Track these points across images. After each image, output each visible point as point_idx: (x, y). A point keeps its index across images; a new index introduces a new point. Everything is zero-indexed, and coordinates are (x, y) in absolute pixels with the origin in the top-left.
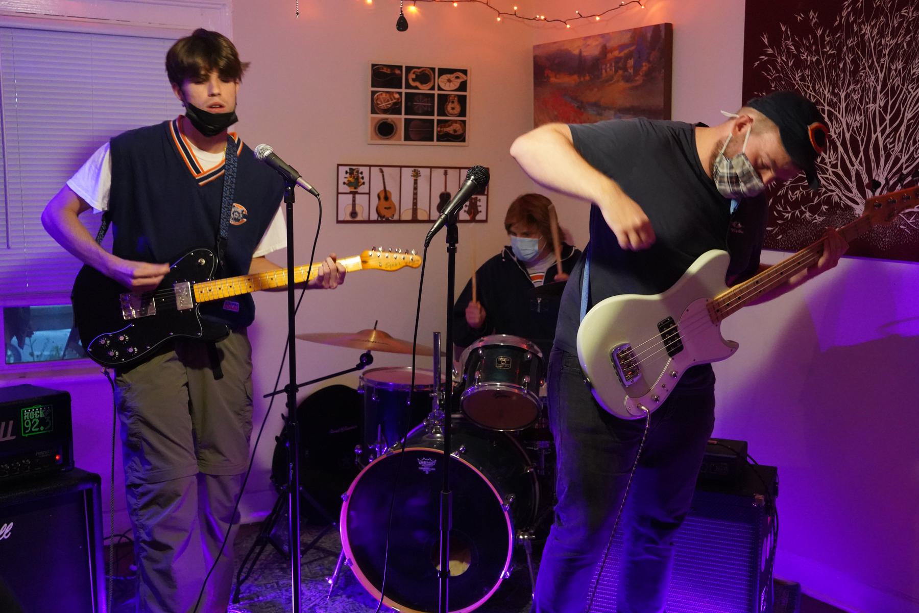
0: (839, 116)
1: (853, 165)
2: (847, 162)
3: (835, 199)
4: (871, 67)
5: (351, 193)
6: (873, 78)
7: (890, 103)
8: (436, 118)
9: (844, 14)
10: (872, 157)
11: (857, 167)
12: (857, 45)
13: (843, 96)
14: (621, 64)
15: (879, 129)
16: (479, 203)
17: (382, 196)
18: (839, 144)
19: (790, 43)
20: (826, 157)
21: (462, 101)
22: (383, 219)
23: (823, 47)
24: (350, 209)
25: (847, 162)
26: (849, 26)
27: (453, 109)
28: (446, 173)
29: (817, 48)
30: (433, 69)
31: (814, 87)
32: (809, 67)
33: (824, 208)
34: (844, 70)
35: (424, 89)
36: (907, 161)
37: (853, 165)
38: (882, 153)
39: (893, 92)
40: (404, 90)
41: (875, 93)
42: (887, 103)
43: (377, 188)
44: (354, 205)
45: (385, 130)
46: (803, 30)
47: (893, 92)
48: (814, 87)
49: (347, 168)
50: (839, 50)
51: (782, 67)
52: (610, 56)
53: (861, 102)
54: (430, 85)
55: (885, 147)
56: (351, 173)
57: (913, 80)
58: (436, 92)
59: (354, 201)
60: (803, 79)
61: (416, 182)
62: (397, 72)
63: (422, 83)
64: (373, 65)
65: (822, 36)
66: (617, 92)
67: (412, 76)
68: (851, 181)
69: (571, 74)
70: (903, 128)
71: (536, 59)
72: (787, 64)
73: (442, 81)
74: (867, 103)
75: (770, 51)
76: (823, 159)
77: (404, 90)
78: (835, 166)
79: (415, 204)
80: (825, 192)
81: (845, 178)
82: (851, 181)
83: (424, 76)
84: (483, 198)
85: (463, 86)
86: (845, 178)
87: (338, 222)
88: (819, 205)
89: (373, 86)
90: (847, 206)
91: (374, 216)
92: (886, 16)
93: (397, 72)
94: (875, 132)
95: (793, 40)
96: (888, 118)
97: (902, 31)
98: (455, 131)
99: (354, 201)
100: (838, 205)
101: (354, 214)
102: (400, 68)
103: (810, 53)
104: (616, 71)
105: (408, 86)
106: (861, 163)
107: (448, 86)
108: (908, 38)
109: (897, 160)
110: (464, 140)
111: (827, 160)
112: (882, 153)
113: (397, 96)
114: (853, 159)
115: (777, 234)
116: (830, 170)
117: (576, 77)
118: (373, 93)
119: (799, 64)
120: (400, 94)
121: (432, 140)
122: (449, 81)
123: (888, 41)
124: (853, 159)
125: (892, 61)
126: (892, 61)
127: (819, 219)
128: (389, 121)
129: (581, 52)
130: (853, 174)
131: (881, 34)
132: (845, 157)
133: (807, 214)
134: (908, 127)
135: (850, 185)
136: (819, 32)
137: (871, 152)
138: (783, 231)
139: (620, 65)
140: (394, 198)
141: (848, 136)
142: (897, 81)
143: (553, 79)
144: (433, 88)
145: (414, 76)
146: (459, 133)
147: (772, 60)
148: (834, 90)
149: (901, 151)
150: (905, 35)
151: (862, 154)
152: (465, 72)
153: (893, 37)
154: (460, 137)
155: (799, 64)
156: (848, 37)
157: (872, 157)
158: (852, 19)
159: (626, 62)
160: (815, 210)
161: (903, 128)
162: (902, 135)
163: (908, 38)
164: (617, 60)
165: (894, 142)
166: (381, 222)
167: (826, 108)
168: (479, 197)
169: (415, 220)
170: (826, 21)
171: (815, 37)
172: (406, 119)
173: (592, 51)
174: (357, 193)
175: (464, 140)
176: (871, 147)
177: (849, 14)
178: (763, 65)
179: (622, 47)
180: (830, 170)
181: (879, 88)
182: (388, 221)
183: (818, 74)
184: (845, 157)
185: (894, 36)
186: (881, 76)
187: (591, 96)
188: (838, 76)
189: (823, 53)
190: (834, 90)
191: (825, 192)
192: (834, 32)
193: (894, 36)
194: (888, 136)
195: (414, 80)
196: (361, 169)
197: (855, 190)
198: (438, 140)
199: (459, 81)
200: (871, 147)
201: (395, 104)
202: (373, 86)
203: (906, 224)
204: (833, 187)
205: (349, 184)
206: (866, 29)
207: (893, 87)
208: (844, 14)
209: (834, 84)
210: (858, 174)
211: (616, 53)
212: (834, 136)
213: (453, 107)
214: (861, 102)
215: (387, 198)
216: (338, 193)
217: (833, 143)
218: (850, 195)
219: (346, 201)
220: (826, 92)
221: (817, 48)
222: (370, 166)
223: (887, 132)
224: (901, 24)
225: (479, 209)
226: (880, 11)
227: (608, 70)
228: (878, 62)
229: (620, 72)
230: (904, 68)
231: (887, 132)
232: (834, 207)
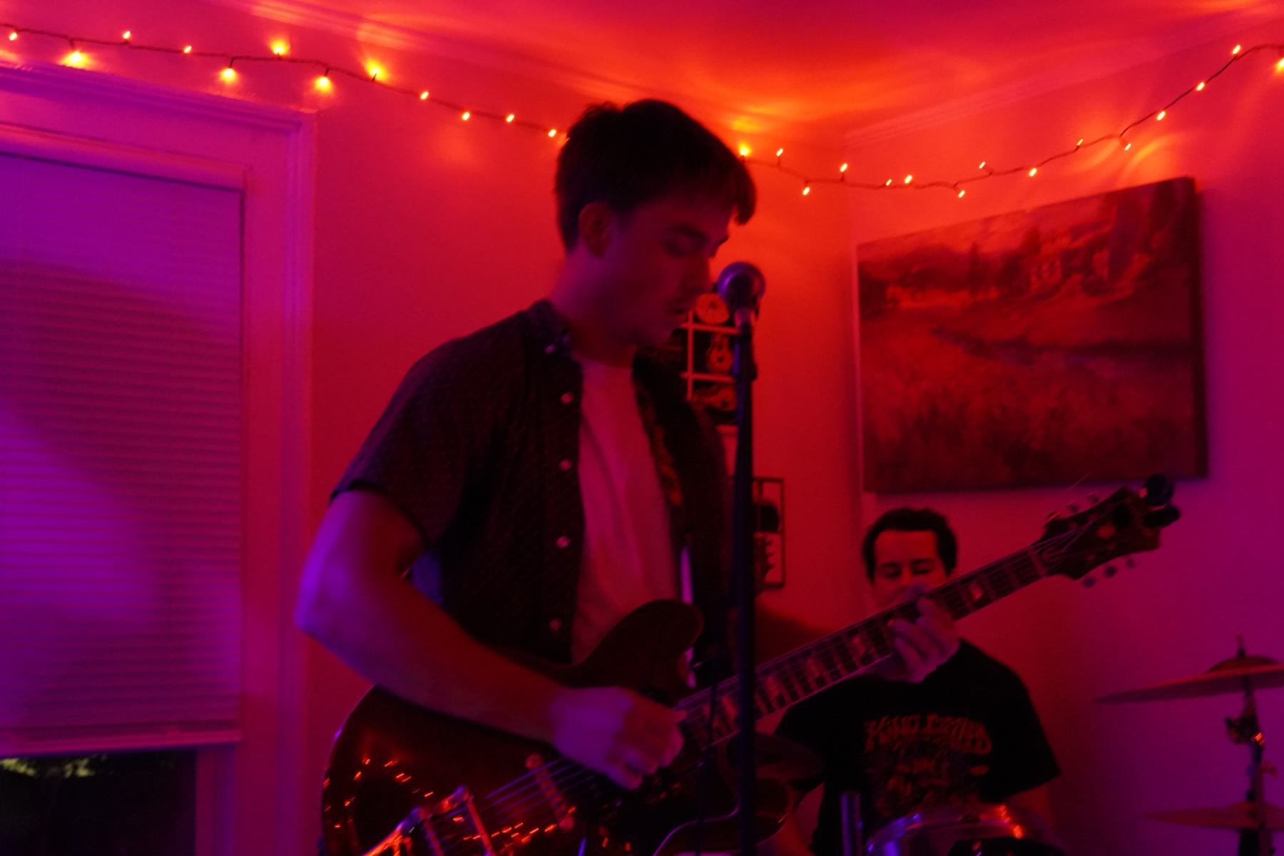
16: (769, 550)
71: (862, 267)
84: (774, 538)
129: (975, 248)
143: (907, 304)
213: (721, 359)
225: (771, 560)
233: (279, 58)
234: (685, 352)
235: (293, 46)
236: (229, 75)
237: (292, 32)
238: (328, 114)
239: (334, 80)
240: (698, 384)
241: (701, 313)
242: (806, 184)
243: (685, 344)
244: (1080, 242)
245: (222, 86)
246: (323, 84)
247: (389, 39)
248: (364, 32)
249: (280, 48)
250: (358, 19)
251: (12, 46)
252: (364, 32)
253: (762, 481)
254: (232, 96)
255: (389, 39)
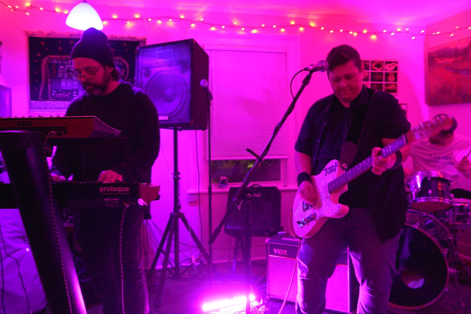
8: (384, 83)
21: (396, 75)
27: (392, 78)
30: (383, 62)
35: (379, 70)
40: (370, 71)
58: (384, 72)
62: (367, 63)
83: (379, 65)
85: (396, 69)
93: (367, 63)
102: (368, 61)
105: (372, 69)
107: (389, 69)
113: (367, 74)
117: (453, 59)
120: (369, 72)
122: (390, 66)
144: (382, 70)
146: (394, 89)
152: (396, 62)
173: (463, 45)
195: (375, 66)
199: (395, 66)
213: (391, 78)
233: (293, 25)
234: (382, 78)
235: (296, 22)
236: (283, 30)
237: (295, 19)
238: (303, 34)
239: (304, 28)
240: (386, 84)
241: (387, 69)
242: (414, 36)
243: (382, 76)
245: (281, 32)
246: (301, 29)
247: (315, 17)
248: (310, 17)
249: (293, 23)
250: (308, 14)
251: (243, 31)
252: (310, 17)
253: (401, 104)
254: (284, 34)
255: (315, 17)
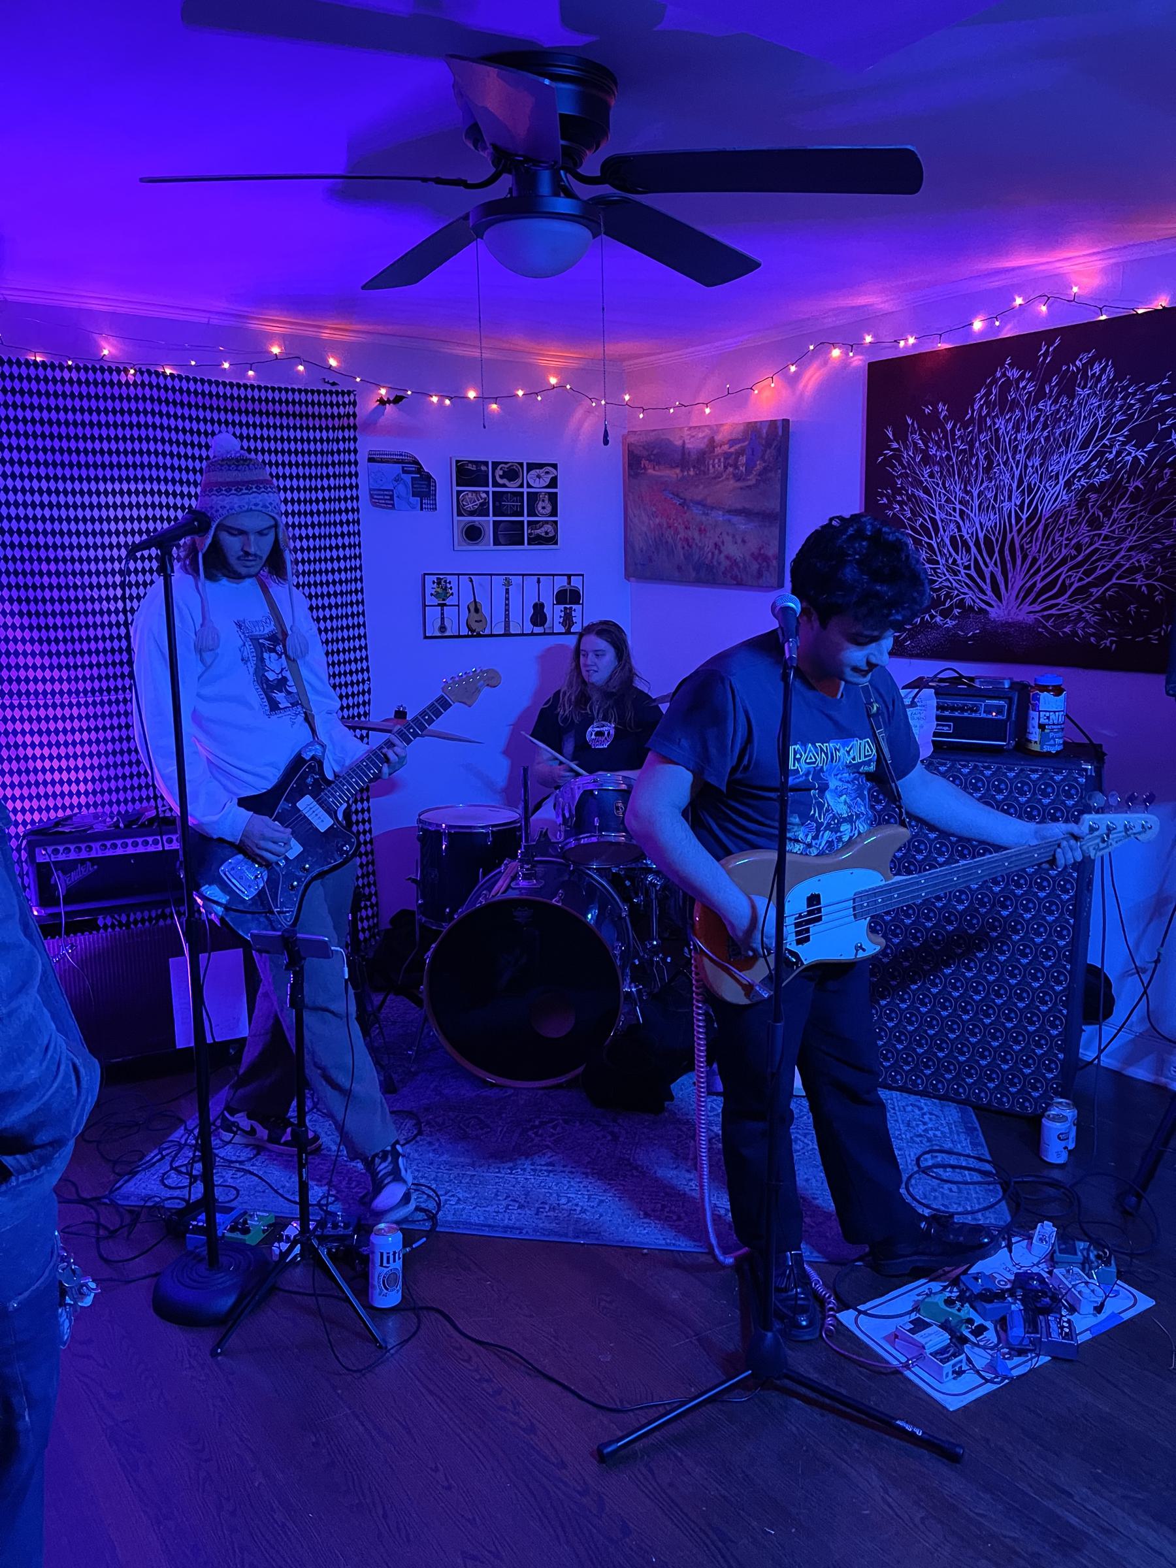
0: (972, 515)
1: (987, 566)
2: (981, 563)
3: (968, 602)
4: (1005, 464)
5: (439, 605)
6: (1008, 475)
7: (1027, 502)
8: (525, 519)
9: (976, 407)
10: (1008, 558)
11: (991, 568)
12: (991, 439)
13: (975, 494)
14: (730, 460)
15: (1015, 529)
17: (472, 609)
18: (971, 545)
19: (917, 437)
20: (958, 558)
21: (553, 498)
22: (474, 634)
23: (954, 441)
24: (438, 624)
25: (981, 563)
26: (982, 419)
28: (539, 581)
29: (947, 443)
30: (521, 464)
31: (944, 484)
32: (938, 463)
33: (956, 611)
34: (976, 466)
35: (512, 487)
36: (1045, 561)
37: (987, 566)
38: (1018, 553)
39: (1030, 491)
40: (491, 489)
41: (1010, 491)
42: (1023, 502)
43: (466, 600)
44: (443, 619)
45: (473, 534)
46: (931, 424)
47: (1030, 491)
48: (944, 484)
49: (434, 578)
50: (971, 444)
51: (908, 462)
52: (718, 450)
53: (995, 500)
54: (519, 482)
55: (1022, 547)
56: (439, 583)
57: (1051, 477)
59: (442, 614)
60: (932, 476)
61: (507, 591)
62: (483, 468)
63: (510, 480)
64: (457, 462)
65: (953, 430)
66: (727, 491)
67: (499, 472)
68: (985, 582)
69: (672, 467)
70: (1041, 527)
72: (914, 459)
73: (530, 477)
74: (1002, 502)
75: (895, 445)
76: (955, 561)
77: (491, 489)
78: (968, 568)
79: (507, 616)
80: (958, 595)
81: (978, 580)
82: (985, 582)
83: (512, 473)
85: (553, 483)
86: (978, 580)
87: (426, 637)
88: (951, 608)
89: (458, 485)
90: (981, 609)
91: (464, 631)
92: (1022, 410)
93: (483, 468)
94: (1011, 531)
95: (921, 434)
96: (1024, 517)
97: (1039, 426)
98: (547, 533)
99: (442, 614)
100: (971, 608)
101: (443, 628)
102: (486, 464)
103: (939, 447)
104: (726, 468)
105: (495, 484)
106: (995, 564)
107: (537, 482)
108: (1045, 434)
109: (1035, 560)
110: (556, 543)
111: (959, 562)
112: (1018, 553)
114: (988, 560)
115: (905, 640)
116: (963, 571)
117: (678, 471)
118: (459, 493)
119: (927, 460)
120: (487, 493)
121: (523, 544)
122: (539, 477)
123: (1024, 436)
124: (988, 560)
125: (1028, 457)
126: (1028, 457)
127: (950, 623)
128: (477, 524)
130: (988, 575)
131: (1017, 428)
132: (979, 558)
133: (938, 619)
134: (1046, 526)
135: (985, 587)
136: (949, 426)
137: (1007, 552)
138: (911, 637)
139: (731, 461)
140: (485, 610)
141: (981, 536)
142: (1035, 479)
143: (650, 471)
144: (521, 486)
145: (501, 473)
146: (550, 535)
147: (898, 456)
148: (965, 487)
149: (1039, 551)
150: (1043, 429)
151: (996, 554)
152: (555, 466)
153: (1030, 432)
154: (553, 540)
155: (927, 460)
156: (980, 432)
157: (1008, 558)
158: (985, 412)
159: (737, 459)
160: (945, 614)
161: (1041, 527)
162: (1040, 535)
163: (1045, 434)
164: (727, 456)
165: (1031, 542)
166: (472, 636)
167: (958, 507)
168: (574, 607)
169: (507, 634)
170: (957, 415)
171: (944, 430)
172: (494, 522)
173: (695, 443)
174: (445, 605)
175: (556, 543)
176: (1007, 547)
177: (982, 406)
178: (888, 460)
179: (732, 442)
180: (963, 571)
181: (1015, 486)
182: (479, 635)
183: (948, 470)
184: (979, 558)
185: (1030, 431)
186: (1017, 473)
187: (699, 493)
188: (970, 473)
189: (954, 448)
190: (965, 487)
191: (958, 595)
192: (965, 426)
193: (1030, 431)
194: (1025, 536)
195: (501, 477)
196: (449, 578)
197: (989, 593)
198: (529, 544)
199: (550, 476)
200: (1007, 547)
201: (481, 504)
202: (458, 485)
203: (1044, 627)
204: (966, 590)
205: (437, 595)
206: (1000, 423)
207: (1029, 485)
208: (976, 407)
209: (966, 482)
210: (992, 574)
211: (726, 447)
212: (967, 536)
213: (543, 506)
214: (995, 500)
215: (477, 610)
216: (425, 606)
217: (965, 543)
218: (984, 598)
219: (433, 613)
220: (957, 490)
221: (947, 443)
222: (459, 575)
223: (1023, 532)
224: (1037, 418)
226: (1015, 404)
227: (716, 466)
228: (1014, 459)
229: (731, 469)
230: (1041, 465)
231: (1023, 532)
232: (967, 610)
237: (284, 339)
244: (732, 450)
255: (339, 336)
